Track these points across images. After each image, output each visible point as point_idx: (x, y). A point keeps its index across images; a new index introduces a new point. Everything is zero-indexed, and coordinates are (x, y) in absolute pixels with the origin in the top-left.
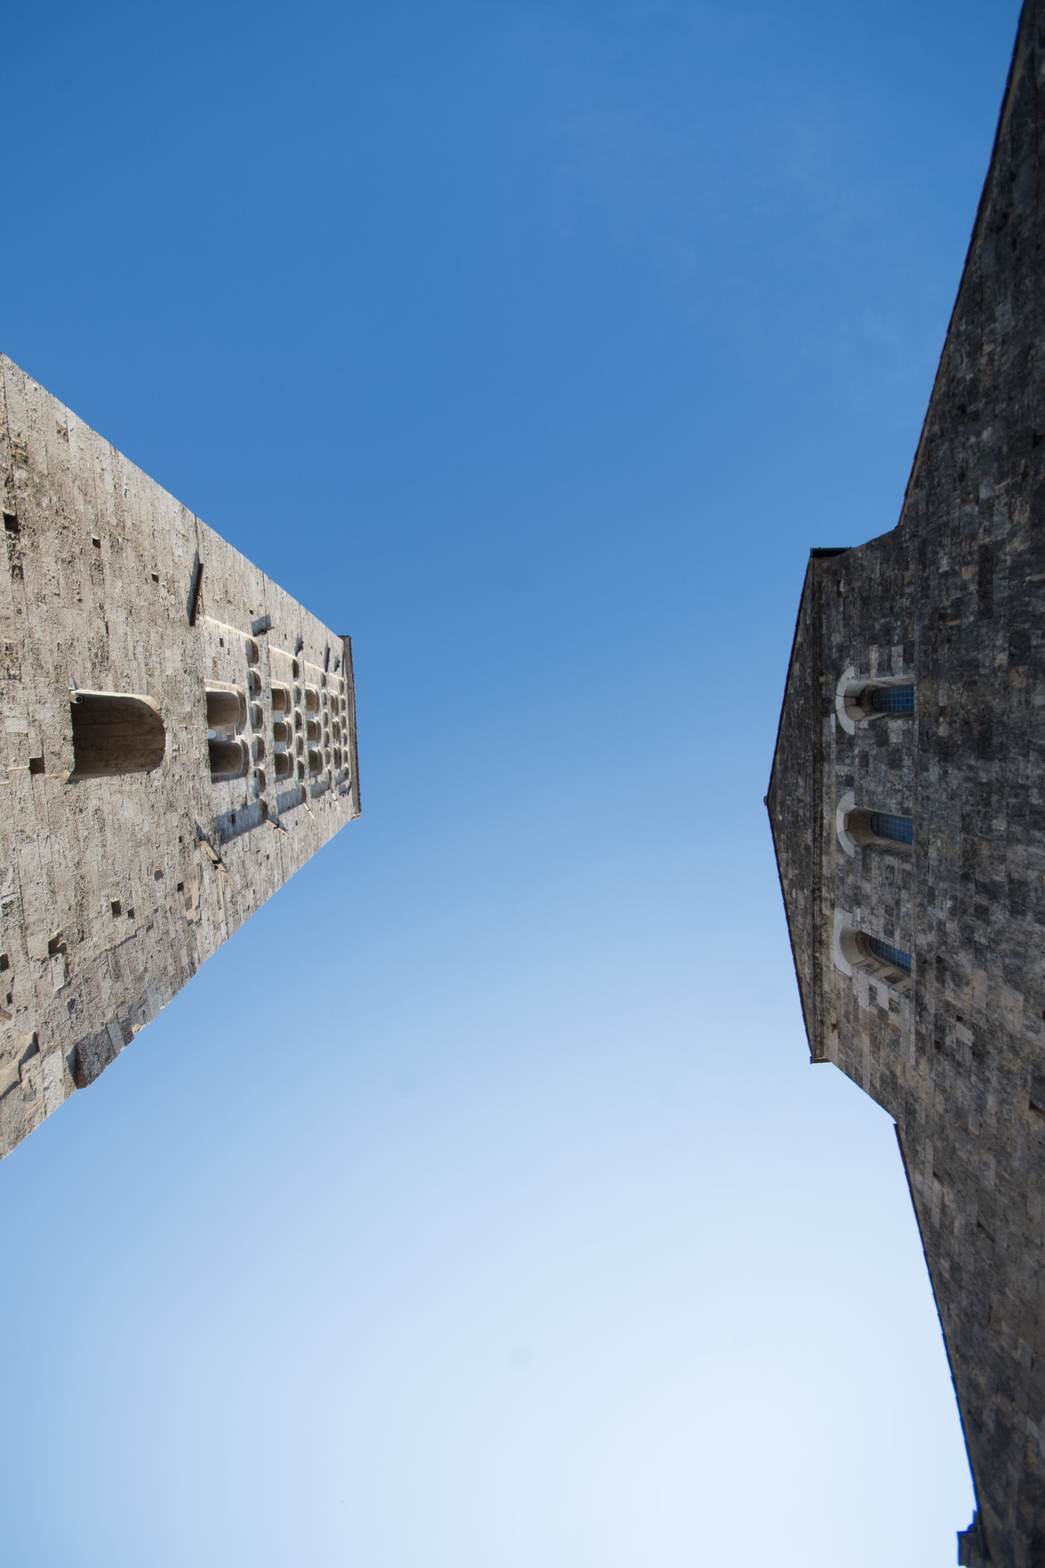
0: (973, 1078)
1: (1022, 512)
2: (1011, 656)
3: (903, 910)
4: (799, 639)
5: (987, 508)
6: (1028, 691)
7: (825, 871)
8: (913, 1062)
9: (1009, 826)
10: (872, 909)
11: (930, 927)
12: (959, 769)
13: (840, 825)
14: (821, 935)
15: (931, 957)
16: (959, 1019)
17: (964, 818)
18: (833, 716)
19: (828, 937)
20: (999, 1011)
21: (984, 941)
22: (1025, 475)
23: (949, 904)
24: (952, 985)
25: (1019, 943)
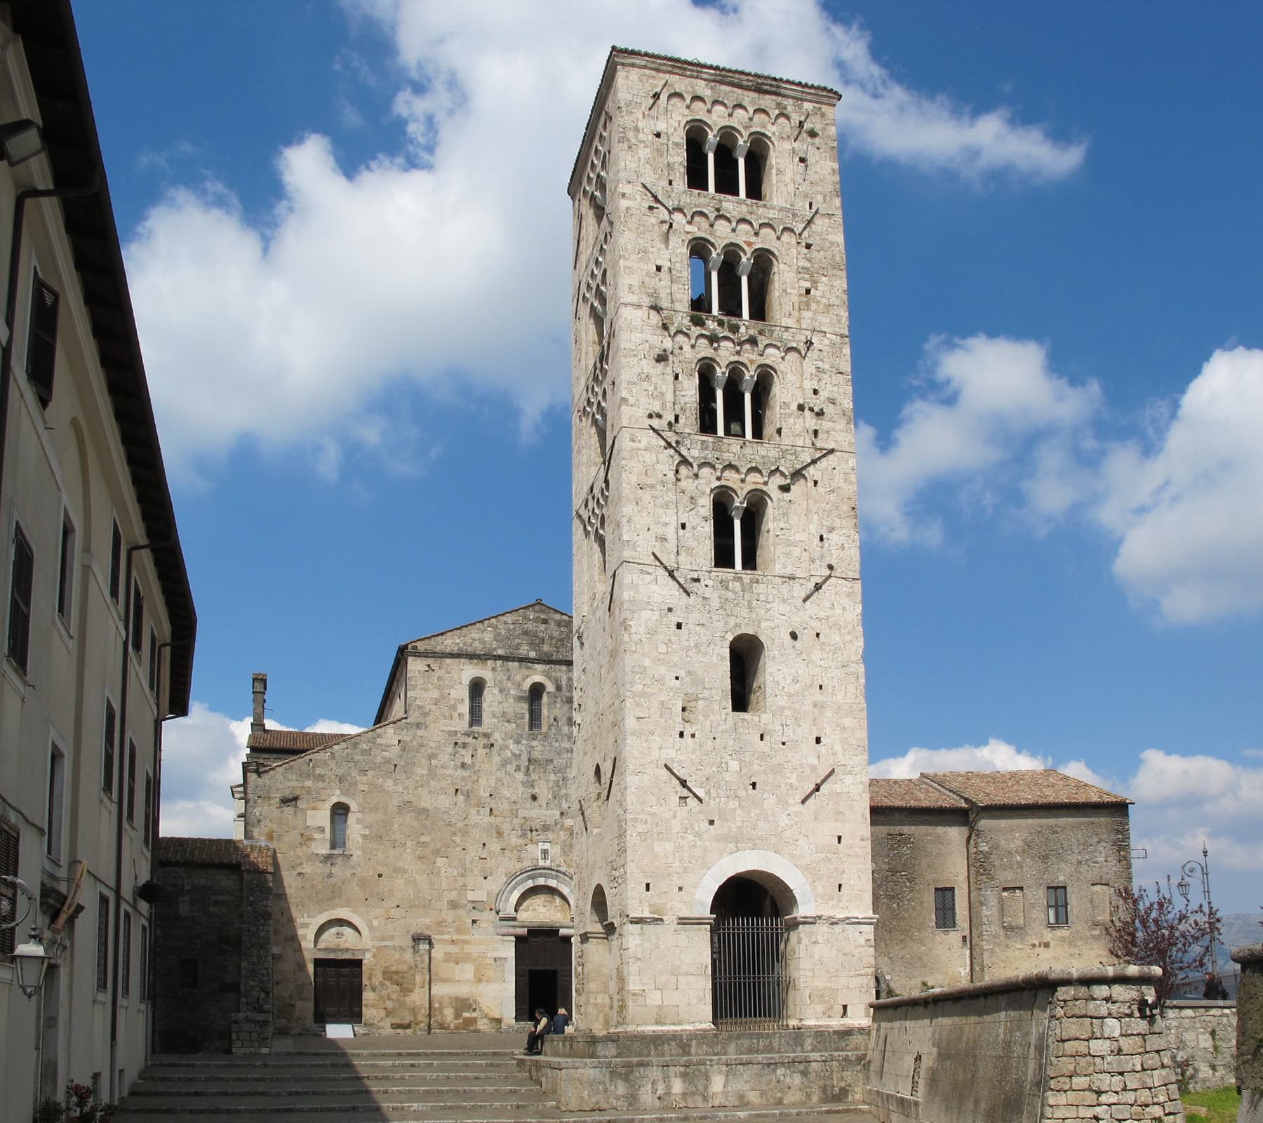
11: (504, 740)
13: (538, 678)
15: (492, 741)
16: (472, 756)
19: (476, 664)
23: (517, 752)
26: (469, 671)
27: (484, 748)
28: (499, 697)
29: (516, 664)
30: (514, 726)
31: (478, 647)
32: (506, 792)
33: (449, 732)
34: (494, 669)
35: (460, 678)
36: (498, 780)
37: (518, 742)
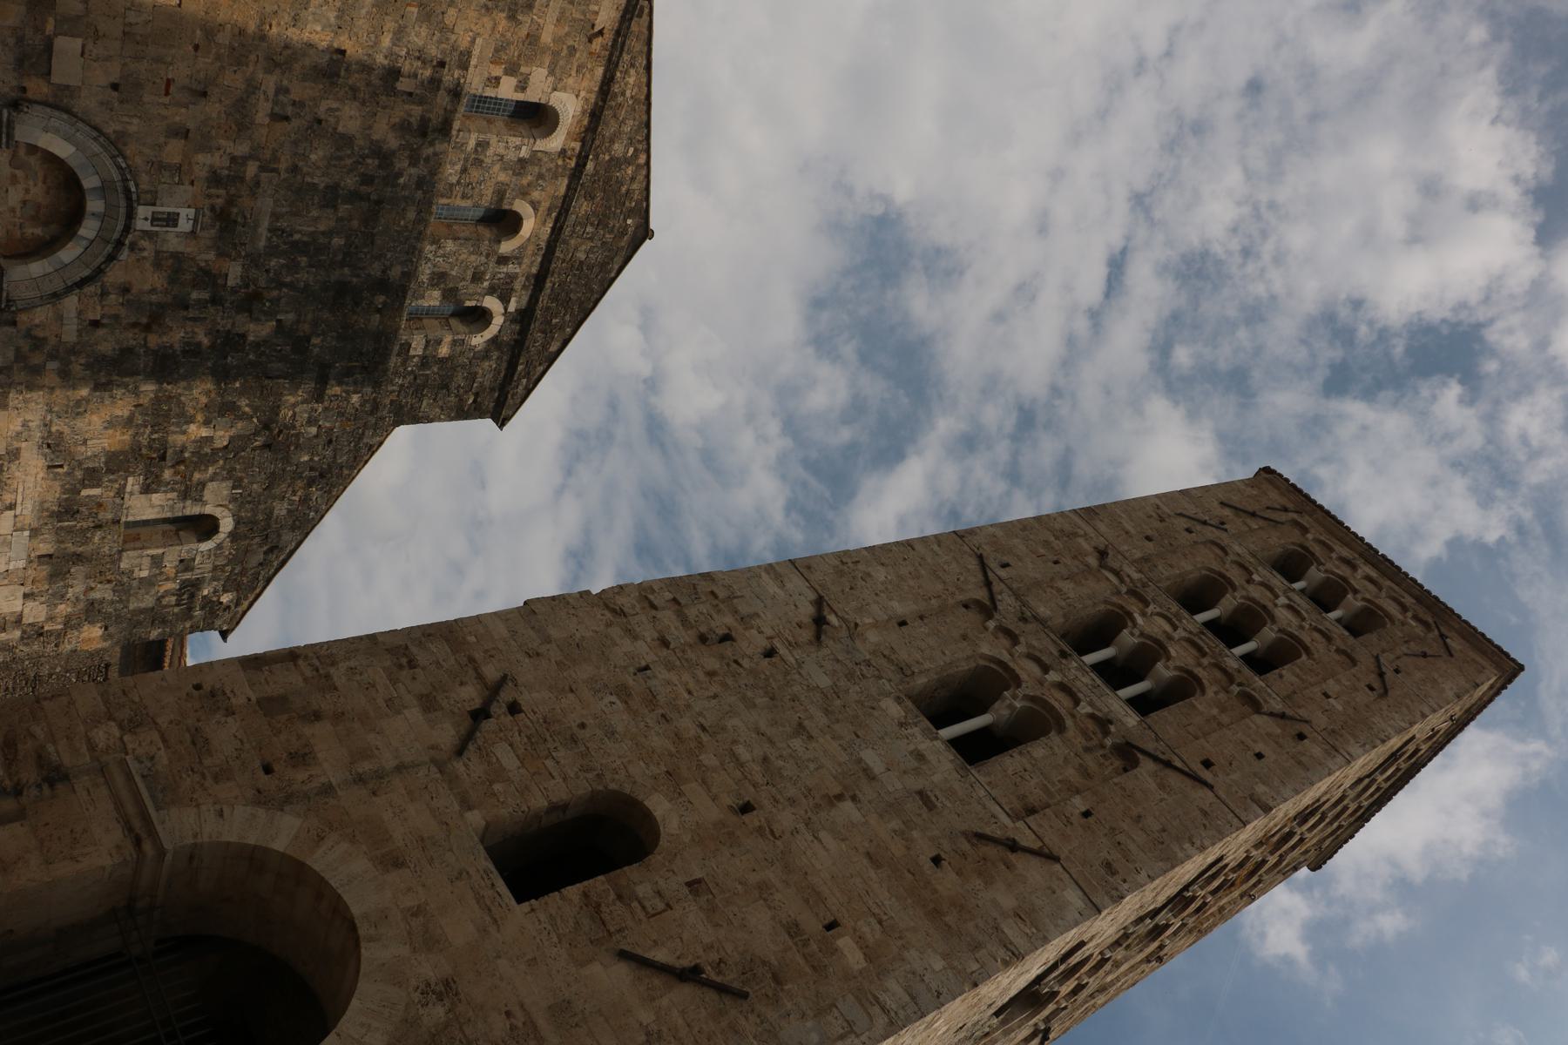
0: (403, 53)
1: (286, 415)
2: (309, 341)
3: (458, 167)
4: (541, 369)
5: (311, 422)
6: (298, 322)
7: (566, 181)
8: (479, 41)
9: (330, 243)
10: (501, 160)
11: (427, 159)
12: (369, 275)
13: (528, 227)
14: (590, 122)
16: (410, 94)
17: (372, 243)
18: (512, 307)
19: (580, 121)
20: (364, 114)
21: (369, 161)
22: (280, 432)
23: (402, 181)
24: (412, 120)
25: (335, 166)
26: (570, 106)
27: (422, 118)
28: (511, 156)
29: (562, 190)
30: (454, 179)
31: (608, 128)
32: (321, 153)
33: (469, 53)
34: (563, 153)
35: (564, 89)
36: (348, 140)
37: (421, 183)
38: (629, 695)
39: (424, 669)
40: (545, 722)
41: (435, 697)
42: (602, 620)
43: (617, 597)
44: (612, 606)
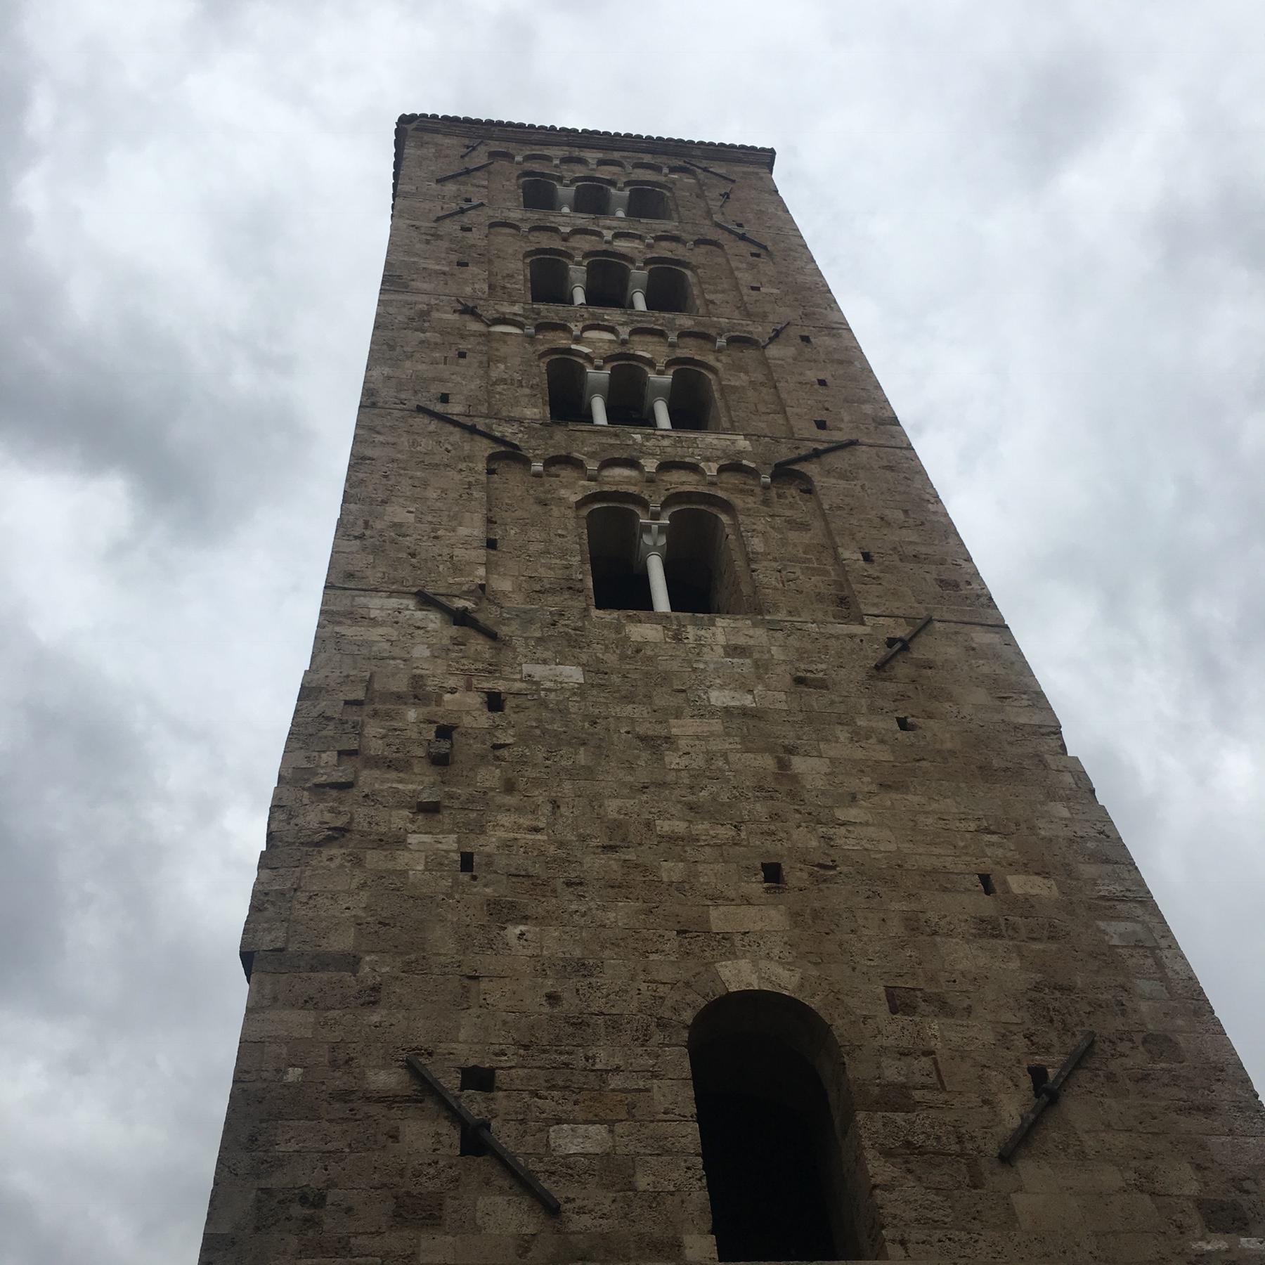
38: (513, 906)
39: (331, 1184)
40: (526, 1047)
41: (408, 1194)
42: (342, 866)
43: (300, 821)
44: (318, 838)
